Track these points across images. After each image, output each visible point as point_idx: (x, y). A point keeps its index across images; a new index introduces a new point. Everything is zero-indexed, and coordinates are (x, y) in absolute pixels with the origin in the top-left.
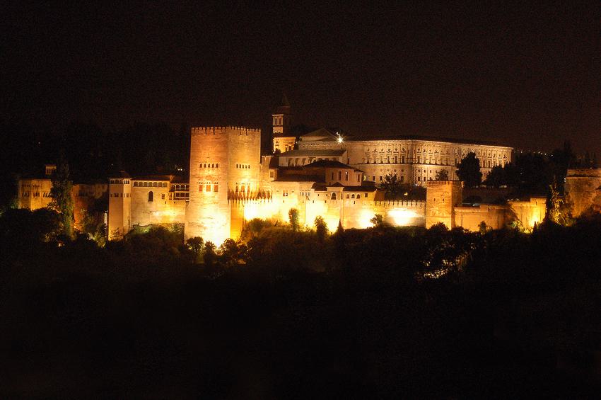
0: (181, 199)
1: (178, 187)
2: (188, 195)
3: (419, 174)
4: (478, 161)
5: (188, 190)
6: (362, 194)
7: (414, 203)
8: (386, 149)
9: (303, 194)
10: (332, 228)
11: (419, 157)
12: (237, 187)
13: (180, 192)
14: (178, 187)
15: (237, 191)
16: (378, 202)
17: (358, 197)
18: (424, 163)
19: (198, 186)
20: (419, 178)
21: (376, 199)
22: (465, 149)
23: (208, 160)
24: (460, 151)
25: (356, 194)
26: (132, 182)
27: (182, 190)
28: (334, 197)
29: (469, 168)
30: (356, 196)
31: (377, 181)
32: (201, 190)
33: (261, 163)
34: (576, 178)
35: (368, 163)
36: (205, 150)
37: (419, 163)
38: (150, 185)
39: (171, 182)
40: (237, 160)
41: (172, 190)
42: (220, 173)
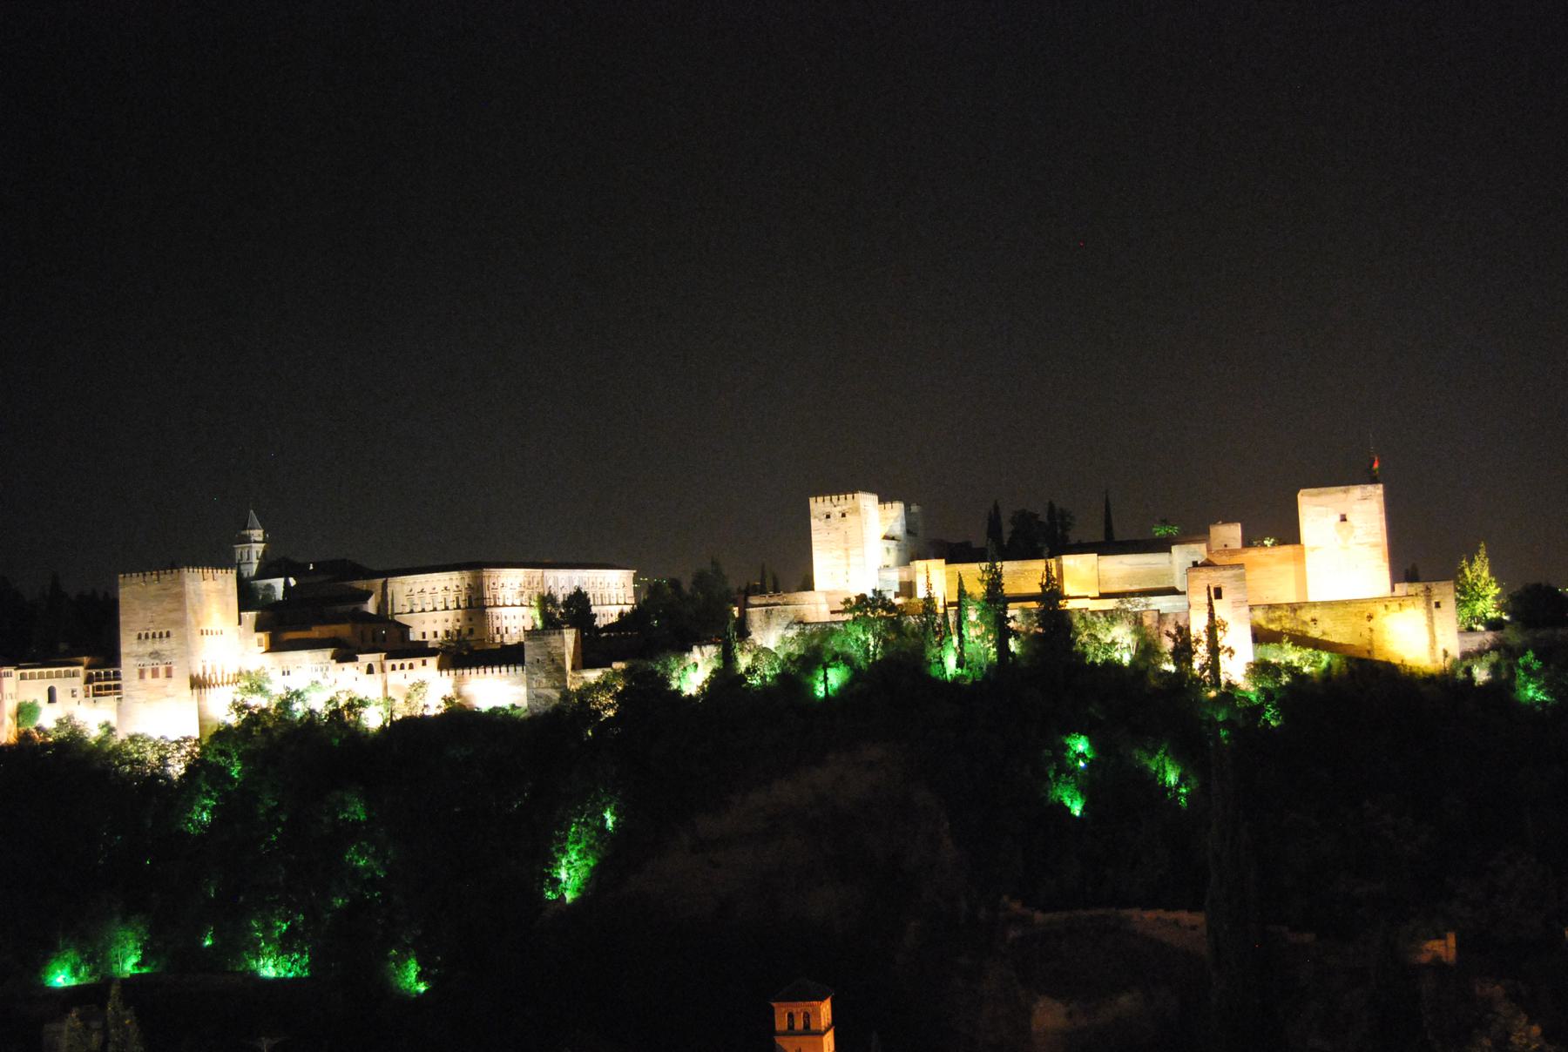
0: (105, 695)
1: (98, 675)
2: (117, 687)
3: (497, 623)
4: (586, 594)
5: (120, 679)
6: (417, 662)
7: (504, 669)
8: (440, 587)
9: (316, 670)
10: (373, 719)
11: (495, 596)
12: (204, 667)
13: (103, 684)
14: (98, 674)
15: (204, 674)
16: (445, 673)
17: (411, 666)
18: (505, 605)
19: (136, 670)
20: (498, 628)
21: (441, 667)
22: (563, 581)
23: (151, 625)
24: (556, 581)
25: (407, 662)
26: (16, 673)
27: (105, 680)
28: (370, 670)
29: (578, 607)
30: (407, 666)
31: (429, 637)
32: (142, 674)
33: (240, 623)
34: (764, 608)
35: (412, 612)
36: (144, 609)
37: (496, 606)
38: (49, 676)
39: (87, 668)
40: (199, 623)
41: (89, 680)
42: (174, 646)
